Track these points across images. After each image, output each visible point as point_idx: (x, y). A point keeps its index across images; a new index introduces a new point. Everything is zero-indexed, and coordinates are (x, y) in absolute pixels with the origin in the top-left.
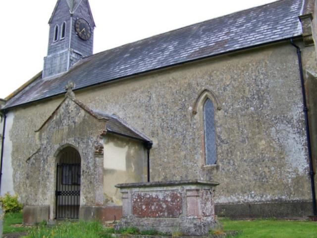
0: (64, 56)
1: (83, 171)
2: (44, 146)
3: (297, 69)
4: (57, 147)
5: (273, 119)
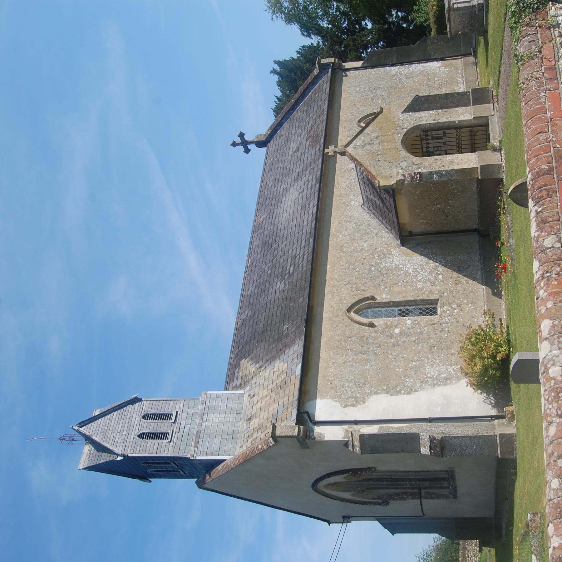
0: (214, 403)
1: (434, 120)
2: (401, 171)
3: (357, 72)
4: (404, 153)
5: (395, 81)
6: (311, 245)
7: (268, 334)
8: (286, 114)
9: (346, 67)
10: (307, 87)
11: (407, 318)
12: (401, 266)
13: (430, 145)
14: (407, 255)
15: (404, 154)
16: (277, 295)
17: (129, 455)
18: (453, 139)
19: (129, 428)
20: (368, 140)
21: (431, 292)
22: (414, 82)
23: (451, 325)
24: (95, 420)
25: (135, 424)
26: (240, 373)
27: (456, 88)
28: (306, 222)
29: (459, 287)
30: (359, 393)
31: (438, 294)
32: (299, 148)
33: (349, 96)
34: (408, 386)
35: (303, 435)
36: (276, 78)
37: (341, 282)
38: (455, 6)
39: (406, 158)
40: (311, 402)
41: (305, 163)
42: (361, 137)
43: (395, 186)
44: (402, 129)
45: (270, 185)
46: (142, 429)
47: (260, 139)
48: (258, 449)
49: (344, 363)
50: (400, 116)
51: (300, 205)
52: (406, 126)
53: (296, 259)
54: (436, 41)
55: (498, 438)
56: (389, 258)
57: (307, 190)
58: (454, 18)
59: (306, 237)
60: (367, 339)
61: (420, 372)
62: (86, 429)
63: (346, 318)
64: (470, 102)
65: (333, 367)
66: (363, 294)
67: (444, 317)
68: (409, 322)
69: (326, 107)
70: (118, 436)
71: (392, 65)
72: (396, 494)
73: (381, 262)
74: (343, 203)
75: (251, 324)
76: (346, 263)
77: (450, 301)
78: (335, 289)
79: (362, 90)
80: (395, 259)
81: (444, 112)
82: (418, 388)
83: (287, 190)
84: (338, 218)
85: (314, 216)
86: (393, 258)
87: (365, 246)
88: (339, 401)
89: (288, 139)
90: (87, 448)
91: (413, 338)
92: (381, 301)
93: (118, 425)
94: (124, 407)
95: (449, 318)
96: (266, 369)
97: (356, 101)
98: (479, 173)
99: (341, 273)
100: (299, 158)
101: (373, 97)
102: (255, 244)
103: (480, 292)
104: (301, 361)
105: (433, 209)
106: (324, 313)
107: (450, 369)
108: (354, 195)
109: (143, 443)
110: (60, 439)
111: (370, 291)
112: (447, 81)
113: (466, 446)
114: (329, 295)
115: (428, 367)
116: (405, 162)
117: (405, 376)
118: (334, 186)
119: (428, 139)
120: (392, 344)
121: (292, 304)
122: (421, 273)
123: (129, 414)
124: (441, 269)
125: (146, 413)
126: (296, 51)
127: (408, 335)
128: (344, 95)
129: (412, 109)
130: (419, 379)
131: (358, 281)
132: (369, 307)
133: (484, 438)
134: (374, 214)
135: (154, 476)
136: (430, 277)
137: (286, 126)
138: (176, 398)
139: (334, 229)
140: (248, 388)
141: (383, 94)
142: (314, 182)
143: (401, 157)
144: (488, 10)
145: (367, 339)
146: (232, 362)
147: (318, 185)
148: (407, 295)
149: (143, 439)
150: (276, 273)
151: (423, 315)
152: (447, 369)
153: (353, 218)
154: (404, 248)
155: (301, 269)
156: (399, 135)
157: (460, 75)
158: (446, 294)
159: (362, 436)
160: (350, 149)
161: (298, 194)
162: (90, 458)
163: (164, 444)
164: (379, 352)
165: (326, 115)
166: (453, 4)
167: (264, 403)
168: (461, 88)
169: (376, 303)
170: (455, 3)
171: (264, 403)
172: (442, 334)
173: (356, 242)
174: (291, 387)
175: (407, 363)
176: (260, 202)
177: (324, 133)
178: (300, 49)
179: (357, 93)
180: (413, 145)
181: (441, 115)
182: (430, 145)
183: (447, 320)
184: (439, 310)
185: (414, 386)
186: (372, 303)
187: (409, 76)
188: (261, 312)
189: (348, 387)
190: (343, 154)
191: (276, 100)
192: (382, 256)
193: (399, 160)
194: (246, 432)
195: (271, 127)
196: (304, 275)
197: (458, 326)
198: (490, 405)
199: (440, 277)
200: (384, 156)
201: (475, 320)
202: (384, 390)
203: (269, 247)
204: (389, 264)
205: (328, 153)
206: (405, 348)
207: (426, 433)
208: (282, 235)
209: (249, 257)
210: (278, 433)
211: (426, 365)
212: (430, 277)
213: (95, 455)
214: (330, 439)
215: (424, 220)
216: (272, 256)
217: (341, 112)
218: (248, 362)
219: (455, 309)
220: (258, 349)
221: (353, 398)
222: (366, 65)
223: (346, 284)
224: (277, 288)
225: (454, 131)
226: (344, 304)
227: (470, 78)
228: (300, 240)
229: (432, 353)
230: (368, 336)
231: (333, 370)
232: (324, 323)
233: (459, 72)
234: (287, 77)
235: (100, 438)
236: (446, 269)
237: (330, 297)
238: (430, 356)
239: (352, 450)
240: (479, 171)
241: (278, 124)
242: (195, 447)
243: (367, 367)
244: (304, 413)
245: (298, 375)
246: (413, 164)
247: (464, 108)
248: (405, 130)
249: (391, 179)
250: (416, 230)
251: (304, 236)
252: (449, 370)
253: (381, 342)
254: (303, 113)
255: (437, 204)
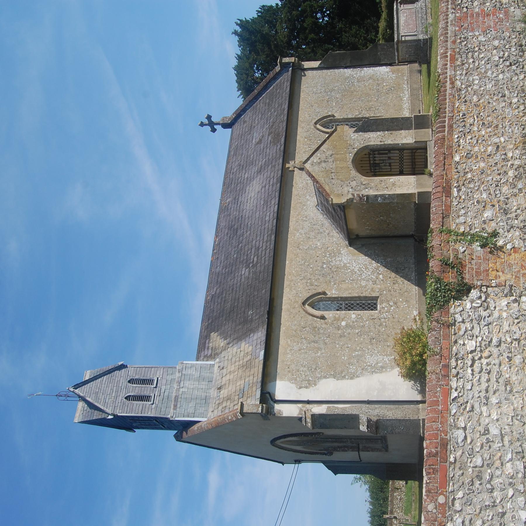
0: (189, 372)
1: (381, 142)
2: (351, 190)
3: (315, 72)
4: (354, 172)
5: (348, 84)
6: (273, 242)
7: (235, 315)
8: (250, 102)
9: (305, 67)
10: (269, 81)
11: (352, 312)
12: (348, 265)
13: (376, 159)
14: (354, 255)
15: (354, 174)
16: (243, 280)
17: (119, 414)
18: (396, 155)
19: (117, 391)
20: (323, 158)
21: (373, 290)
22: (365, 86)
23: (388, 321)
24: (88, 383)
25: (123, 388)
26: (211, 345)
27: (401, 95)
28: (268, 218)
29: (396, 287)
30: (312, 377)
31: (378, 292)
32: (261, 140)
33: (307, 96)
34: (351, 372)
35: (266, 412)
36: (237, 38)
37: (298, 277)
38: (403, 39)
39: (356, 177)
40: (272, 383)
41: (267, 158)
42: (318, 154)
43: (345, 204)
44: (353, 148)
45: (235, 170)
46: (128, 392)
47: (226, 122)
48: (228, 419)
49: (300, 350)
50: (352, 136)
51: (263, 199)
52: (356, 145)
53: (259, 251)
54: (385, 47)
55: (421, 422)
56: (338, 257)
57: (269, 186)
58: (402, 49)
59: (268, 233)
60: (318, 330)
61: (361, 360)
62: (80, 391)
63: (301, 310)
64: (412, 126)
65: (291, 354)
66: (316, 289)
67: (383, 313)
68: (353, 316)
69: (286, 107)
70: (108, 398)
71: (346, 68)
72: (339, 447)
73: (332, 261)
74: (301, 203)
75: (219, 301)
76: (302, 260)
77: (388, 299)
78: (292, 283)
79: (319, 91)
80: (343, 259)
81: (389, 135)
82: (359, 374)
83: (250, 180)
84: (296, 217)
85: (275, 215)
86: (342, 257)
87: (319, 244)
88: (295, 383)
89: (251, 128)
90: (81, 405)
91: (357, 331)
92: (331, 296)
93: (107, 388)
94: (112, 372)
95: (387, 314)
96: (234, 346)
97: (313, 103)
98: (417, 198)
99: (297, 269)
100: (262, 151)
101: (328, 99)
102: (223, 224)
103: (413, 291)
104: (264, 348)
105: (377, 220)
106: (283, 305)
107: (386, 359)
108: (310, 196)
109: (129, 405)
110: (56, 396)
111: (321, 287)
112: (394, 87)
113: (395, 427)
114: (287, 288)
115: (368, 357)
116: (355, 182)
117: (349, 364)
118: (292, 186)
119: (375, 154)
120: (339, 335)
121: (256, 293)
122: (365, 272)
123: (117, 378)
124: (382, 269)
125: (131, 378)
126: (257, 11)
127: (353, 327)
128: (302, 95)
129: (363, 130)
130: (360, 367)
131: (312, 277)
132: (321, 300)
133: (410, 421)
134: (326, 215)
135: (138, 428)
136: (372, 276)
137: (249, 113)
138: (157, 366)
139: (292, 227)
140: (218, 360)
141: (337, 96)
142: (275, 180)
143: (351, 176)
144: (431, 47)
145: (318, 330)
146: (203, 332)
147: (279, 185)
148: (353, 291)
149: (129, 400)
150: (242, 259)
151: (365, 310)
152: (383, 359)
153: (309, 218)
154: (352, 248)
155: (263, 262)
156: (350, 155)
157: (406, 82)
158: (385, 292)
159: (313, 416)
160: (307, 166)
161: (261, 187)
162: (84, 414)
163: (147, 406)
164: (328, 342)
165: (286, 115)
166: (402, 36)
167: (232, 377)
168: (406, 114)
169: (327, 297)
170: (403, 36)
171: (232, 377)
172: (380, 328)
173: (311, 240)
174: (255, 369)
175: (351, 352)
176: (226, 184)
177: (284, 134)
178: (260, 8)
179: (314, 94)
180: (361, 161)
181: (387, 137)
182: (376, 159)
183: (385, 316)
184: (378, 306)
185: (356, 373)
186: (324, 297)
187: (361, 80)
188: (228, 293)
189: (303, 371)
190: (302, 169)
191: (236, 56)
192: (333, 254)
193: (349, 179)
194: (217, 399)
195: (236, 111)
196: (266, 268)
197: (393, 322)
198: (417, 391)
199: (381, 276)
200: (337, 174)
201: (408, 317)
202: (332, 375)
203: (235, 231)
204: (338, 263)
205: (289, 168)
206: (350, 339)
207: (365, 415)
208: (246, 224)
209: (217, 236)
210: (245, 410)
211: (366, 355)
212: (372, 276)
213: (89, 412)
214: (287, 416)
215: (369, 227)
216: (237, 241)
217: (300, 112)
218: (217, 336)
219: (392, 306)
220: (226, 327)
221: (306, 381)
222: (322, 65)
223: (302, 279)
224: (243, 274)
225: (398, 152)
226: (300, 297)
227: (415, 86)
228: (263, 234)
229: (372, 344)
230: (319, 327)
231: (290, 356)
232: (283, 314)
233: (405, 78)
234: (248, 39)
235: (93, 399)
236: (386, 269)
237: (288, 290)
238: (370, 347)
239: (305, 425)
240: (416, 196)
241: (242, 110)
242: (174, 409)
243: (319, 354)
244: (266, 393)
245: (261, 360)
246: (362, 184)
247: (407, 131)
248: (356, 150)
249: (342, 197)
250: (362, 233)
251: (266, 232)
252: (385, 360)
253: (330, 333)
254: (266, 106)
255: (381, 216)
